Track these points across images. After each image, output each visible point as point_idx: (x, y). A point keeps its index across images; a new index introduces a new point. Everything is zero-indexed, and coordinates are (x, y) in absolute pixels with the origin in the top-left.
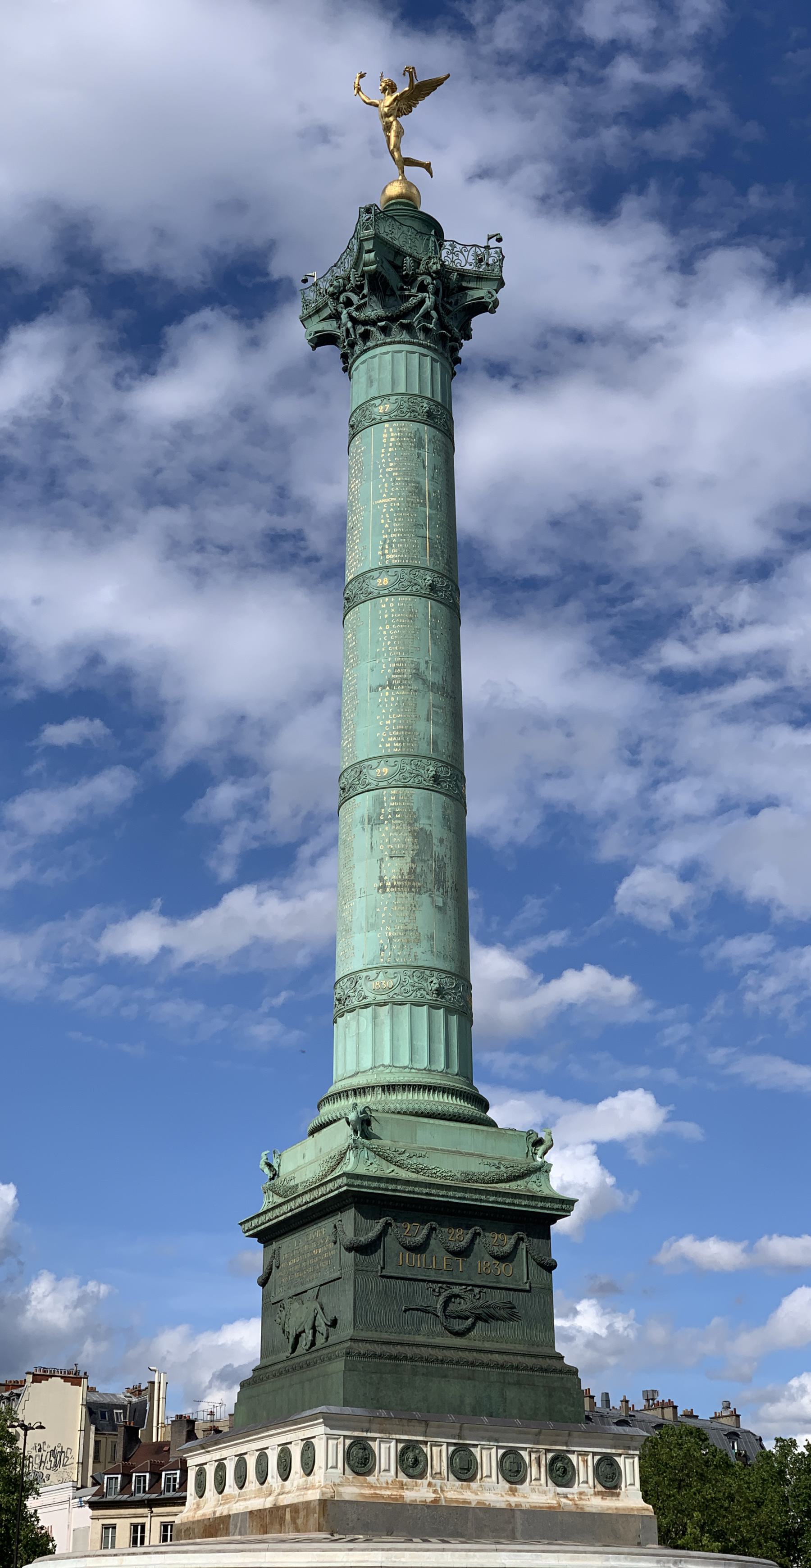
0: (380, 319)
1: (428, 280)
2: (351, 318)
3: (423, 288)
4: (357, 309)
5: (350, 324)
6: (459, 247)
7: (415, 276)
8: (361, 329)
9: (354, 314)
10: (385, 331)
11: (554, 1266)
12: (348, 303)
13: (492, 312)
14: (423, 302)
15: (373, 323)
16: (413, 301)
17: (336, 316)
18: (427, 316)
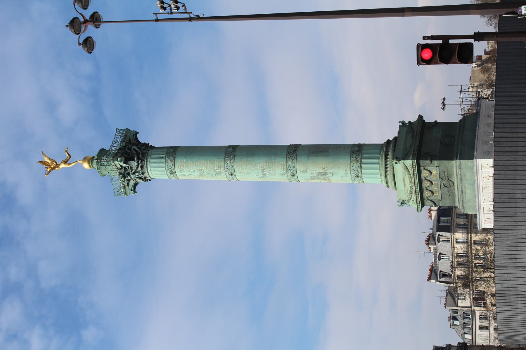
0: (138, 162)
1: (127, 147)
2: (134, 174)
3: (130, 149)
4: (131, 171)
5: (136, 174)
6: (115, 140)
7: (126, 151)
8: (139, 169)
9: (133, 171)
10: (142, 161)
11: (436, 121)
12: (129, 174)
13: (138, 133)
14: (134, 149)
15: (138, 164)
16: (134, 152)
17: (129, 180)
18: (139, 148)
